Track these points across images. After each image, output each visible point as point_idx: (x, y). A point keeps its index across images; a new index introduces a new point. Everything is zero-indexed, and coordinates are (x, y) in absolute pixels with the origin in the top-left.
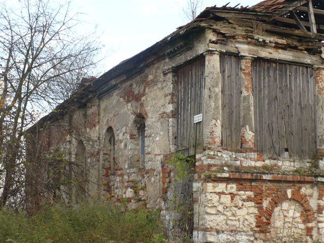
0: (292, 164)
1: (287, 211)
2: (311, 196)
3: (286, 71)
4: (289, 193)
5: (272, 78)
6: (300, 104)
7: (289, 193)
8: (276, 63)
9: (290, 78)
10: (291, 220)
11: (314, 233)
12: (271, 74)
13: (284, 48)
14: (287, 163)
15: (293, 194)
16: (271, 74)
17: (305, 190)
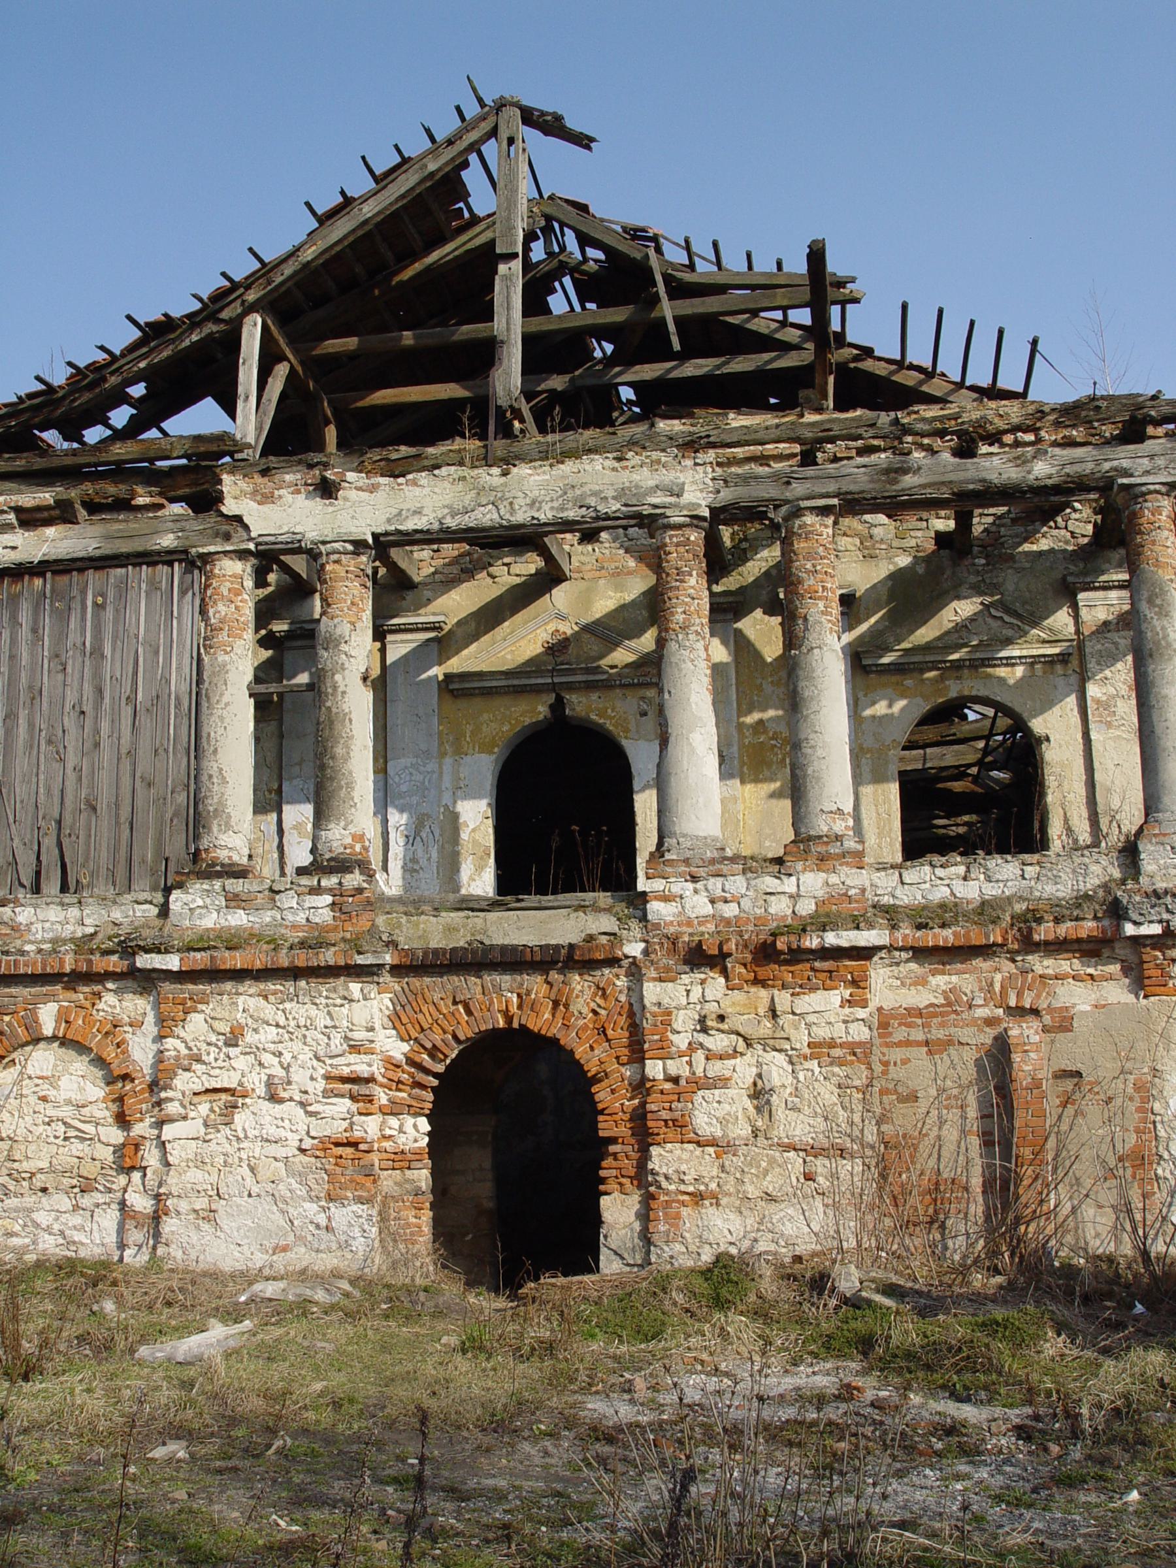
0: (74, 912)
1: (51, 1080)
2: (136, 1024)
3: (84, 592)
4: (48, 1017)
5: (25, 632)
6: (131, 700)
7: (48, 1017)
8: (42, 574)
9: (96, 616)
10: (66, 1112)
11: (151, 1157)
12: (25, 617)
13: (62, 514)
14: (54, 914)
15: (63, 1018)
16: (25, 617)
17: (116, 1004)
